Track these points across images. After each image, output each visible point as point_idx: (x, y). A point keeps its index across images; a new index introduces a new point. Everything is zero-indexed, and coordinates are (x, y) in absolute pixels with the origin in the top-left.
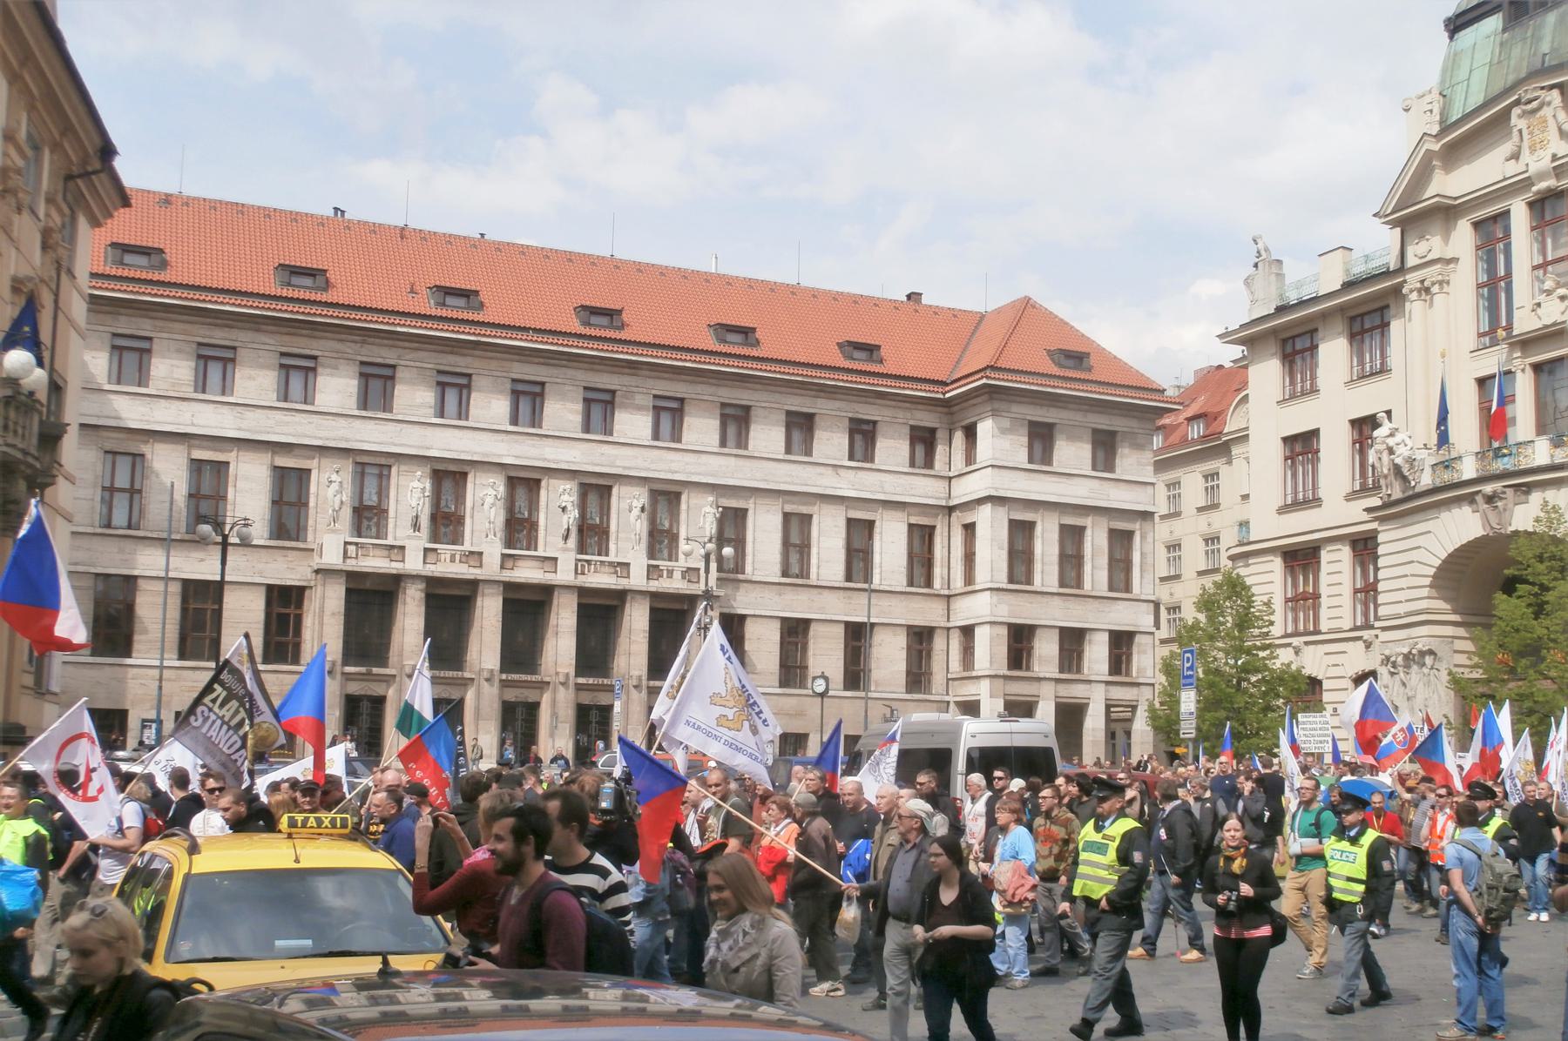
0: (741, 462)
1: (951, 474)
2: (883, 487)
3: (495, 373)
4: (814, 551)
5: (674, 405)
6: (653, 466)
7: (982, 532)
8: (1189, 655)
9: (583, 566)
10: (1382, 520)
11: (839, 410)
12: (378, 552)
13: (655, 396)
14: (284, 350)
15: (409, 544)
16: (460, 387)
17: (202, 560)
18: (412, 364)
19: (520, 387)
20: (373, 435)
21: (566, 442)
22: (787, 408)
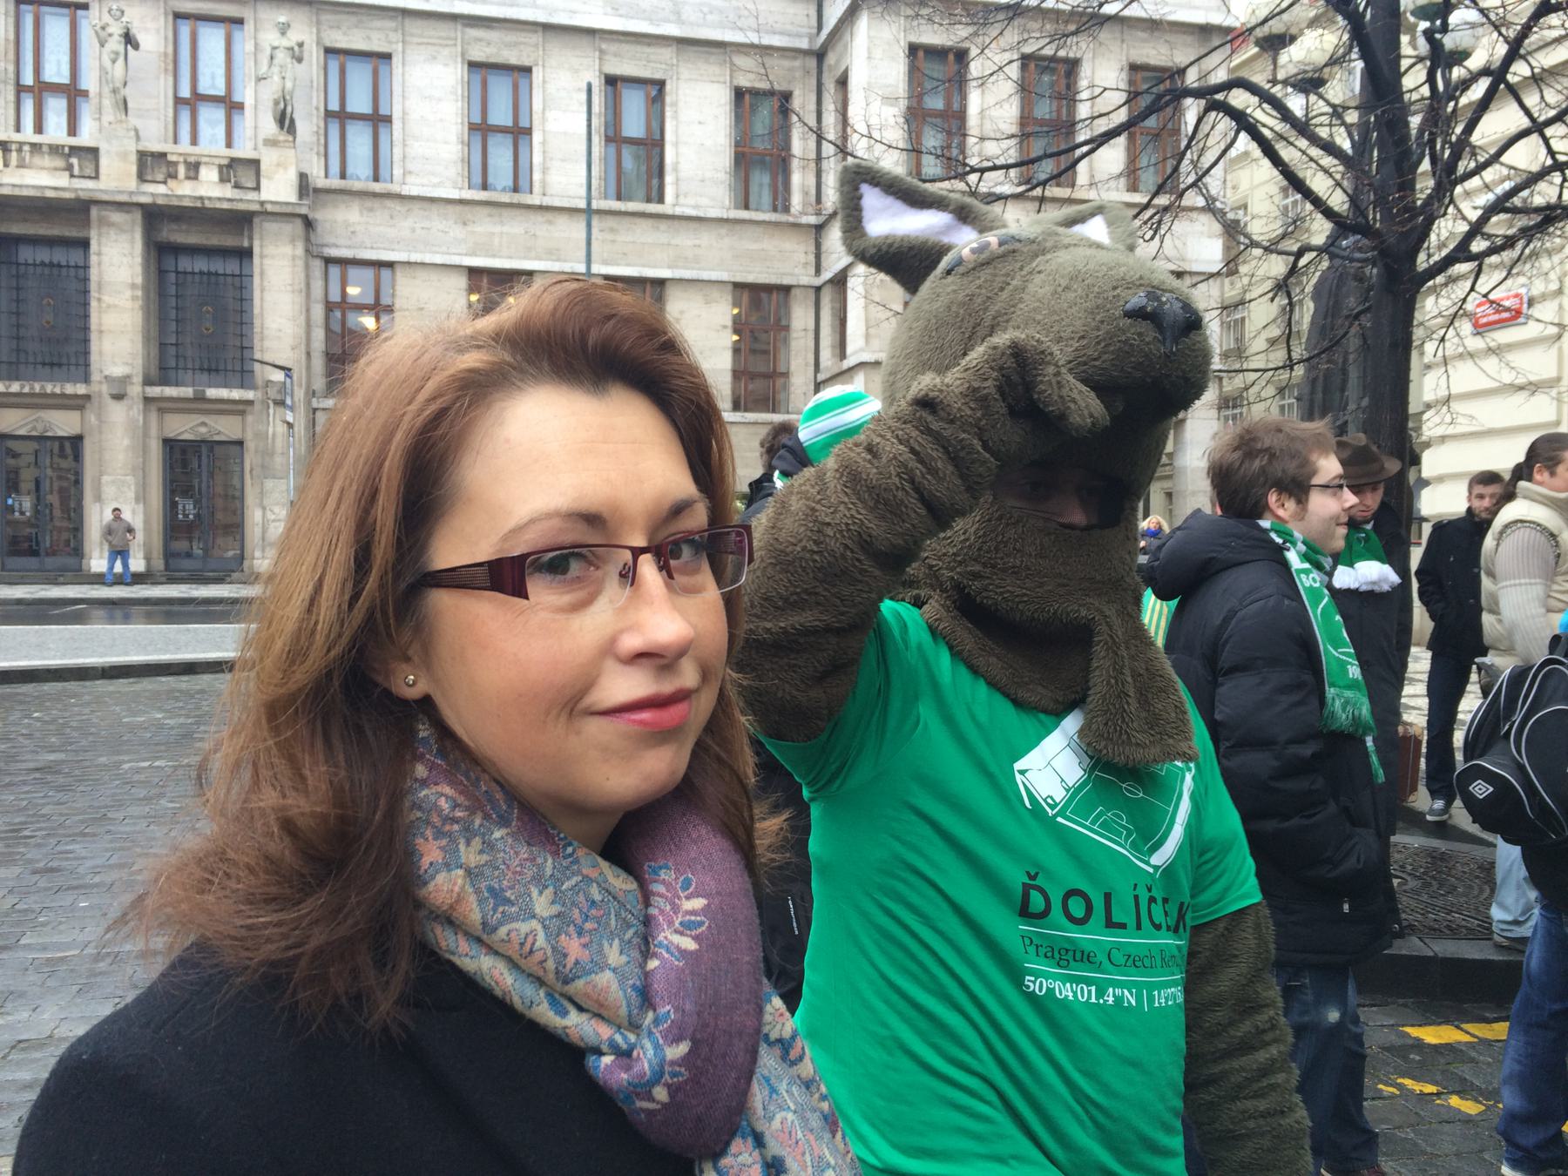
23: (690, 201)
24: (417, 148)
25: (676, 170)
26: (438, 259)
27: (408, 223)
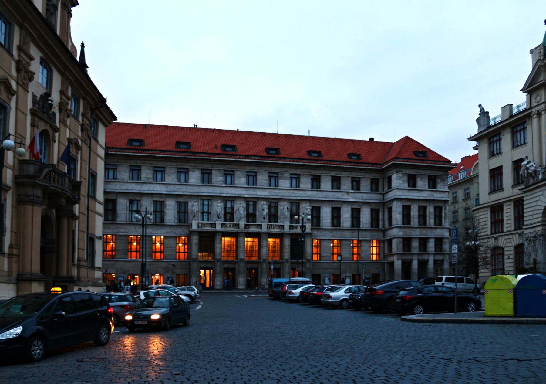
0: (318, 193)
1: (384, 192)
2: (362, 198)
3: (241, 170)
4: (341, 218)
5: (297, 176)
6: (291, 195)
7: (393, 209)
8: (455, 231)
9: (270, 226)
10: (524, 192)
11: (348, 175)
12: (208, 225)
13: (291, 174)
14: (179, 167)
15: (217, 222)
16: (231, 175)
17: (158, 230)
18: (216, 168)
19: (248, 174)
20: (206, 191)
21: (264, 190)
22: (332, 175)
23: (365, 227)
24: (324, 221)
25: (362, 222)
26: (327, 238)
27: (323, 233)
